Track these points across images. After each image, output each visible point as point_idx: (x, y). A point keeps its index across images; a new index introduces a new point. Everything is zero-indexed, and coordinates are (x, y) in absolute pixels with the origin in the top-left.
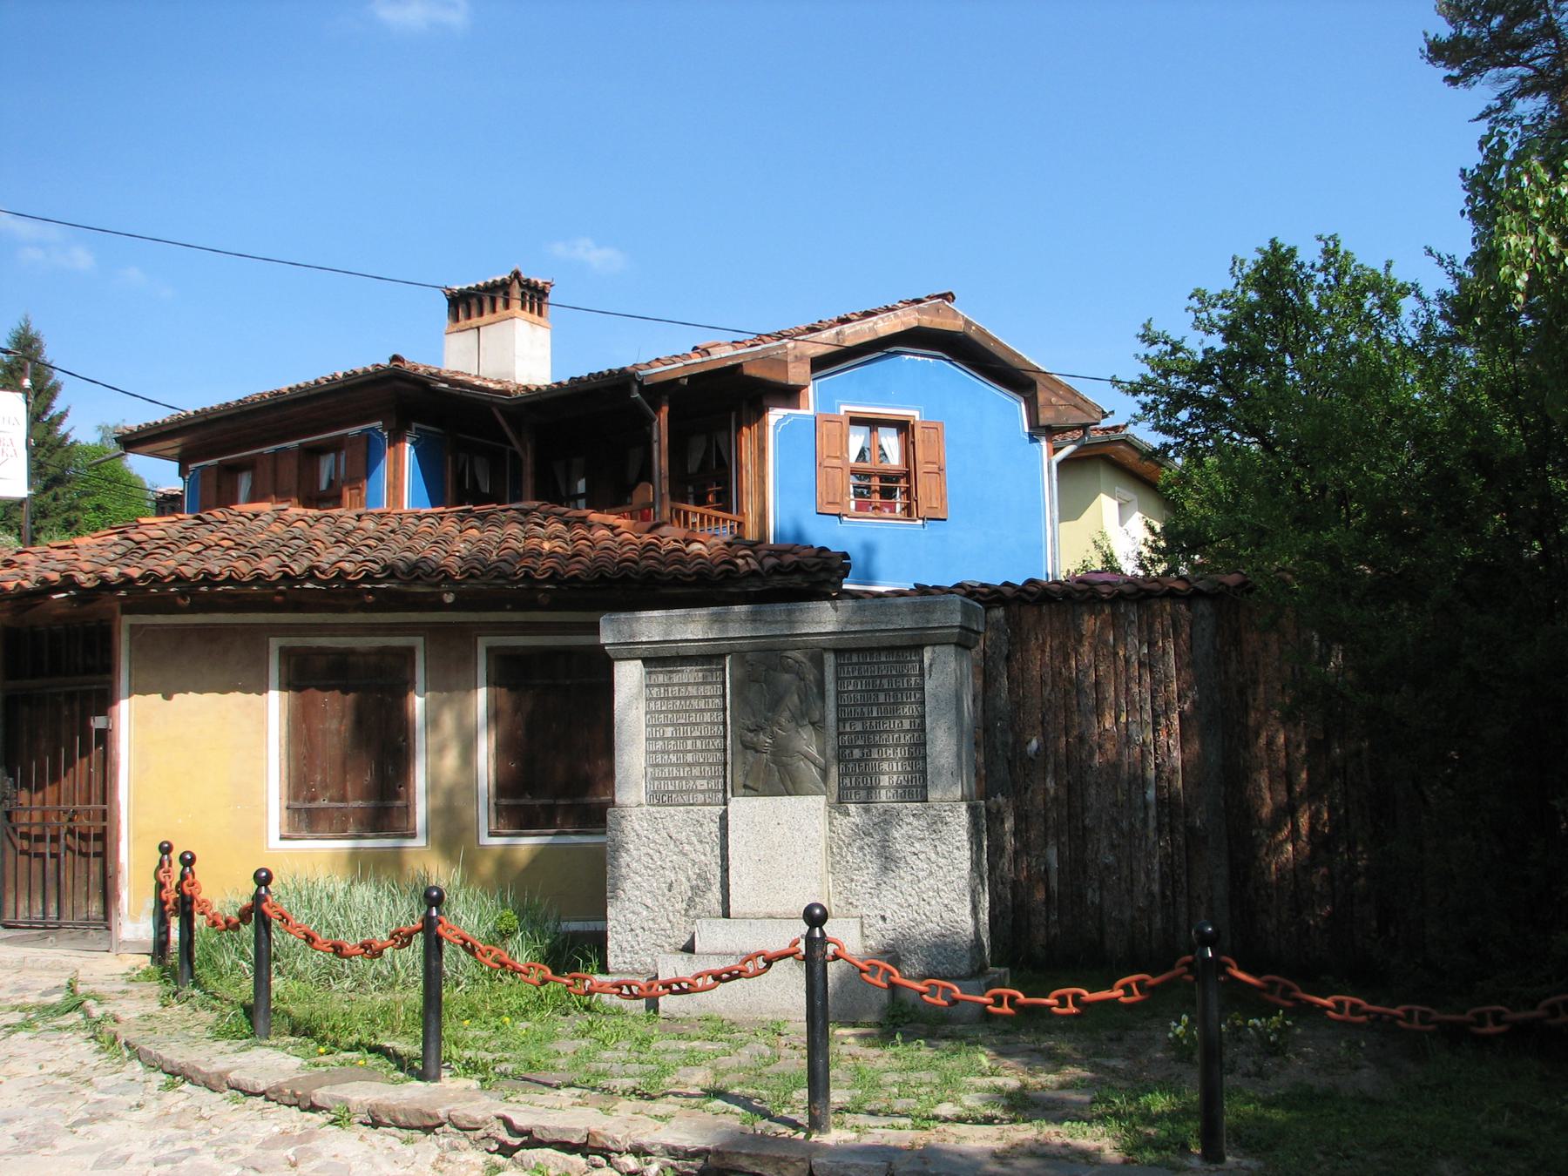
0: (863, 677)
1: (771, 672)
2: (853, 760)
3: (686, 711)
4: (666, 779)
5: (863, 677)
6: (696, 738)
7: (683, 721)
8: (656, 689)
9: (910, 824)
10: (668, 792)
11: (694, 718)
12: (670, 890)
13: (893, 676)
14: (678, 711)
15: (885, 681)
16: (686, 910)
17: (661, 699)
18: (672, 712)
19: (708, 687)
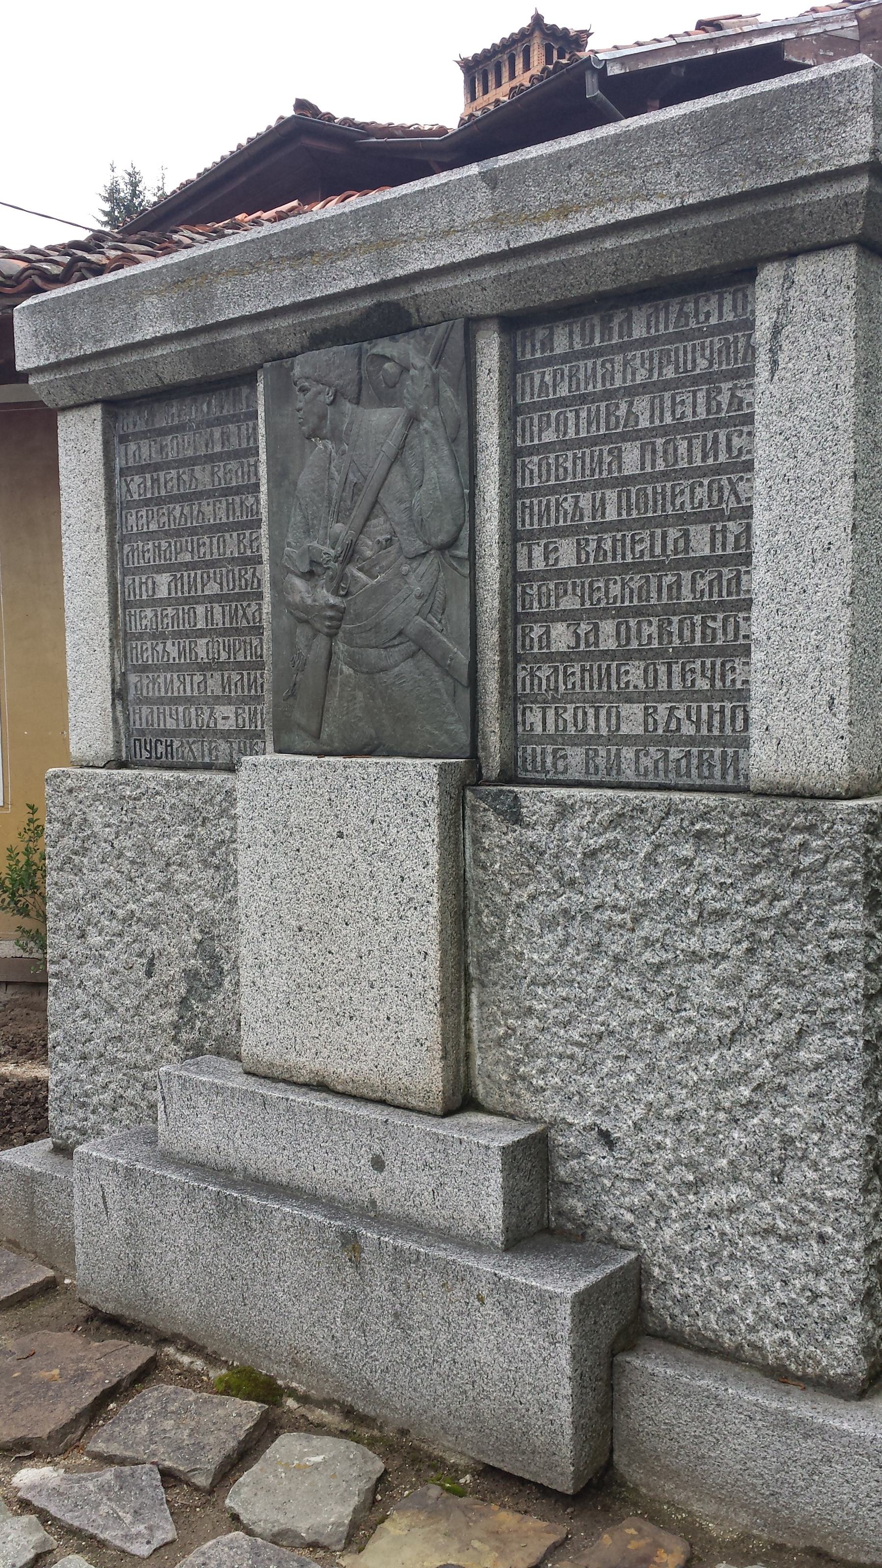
0: (583, 399)
1: (348, 407)
2: (550, 657)
3: (193, 531)
4: (160, 701)
5: (583, 399)
6: (211, 599)
7: (188, 558)
8: (137, 479)
9: (688, 862)
10: (165, 732)
11: (210, 548)
12: (149, 974)
13: (666, 385)
14: (178, 533)
15: (642, 404)
16: (176, 1027)
17: (147, 503)
18: (167, 534)
19: (233, 465)
